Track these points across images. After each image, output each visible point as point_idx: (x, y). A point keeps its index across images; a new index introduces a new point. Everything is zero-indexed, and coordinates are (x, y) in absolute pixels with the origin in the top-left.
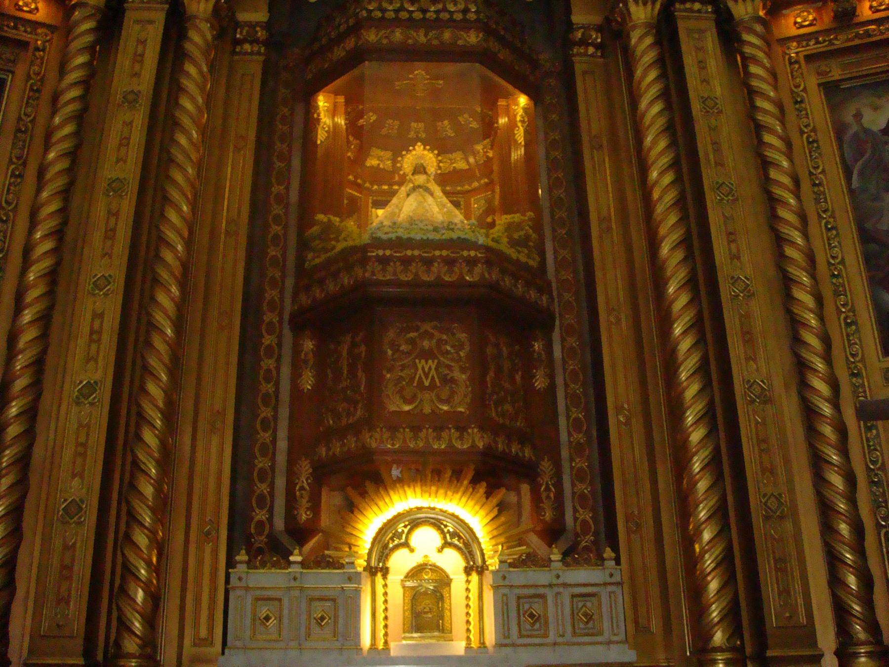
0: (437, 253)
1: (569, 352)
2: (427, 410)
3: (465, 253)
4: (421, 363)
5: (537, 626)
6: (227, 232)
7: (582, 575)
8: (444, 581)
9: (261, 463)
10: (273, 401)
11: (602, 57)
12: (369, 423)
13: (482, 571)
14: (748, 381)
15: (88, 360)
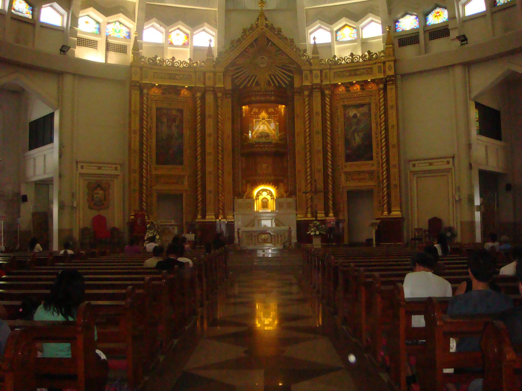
8: (268, 200)
11: (300, 95)
13: (273, 199)
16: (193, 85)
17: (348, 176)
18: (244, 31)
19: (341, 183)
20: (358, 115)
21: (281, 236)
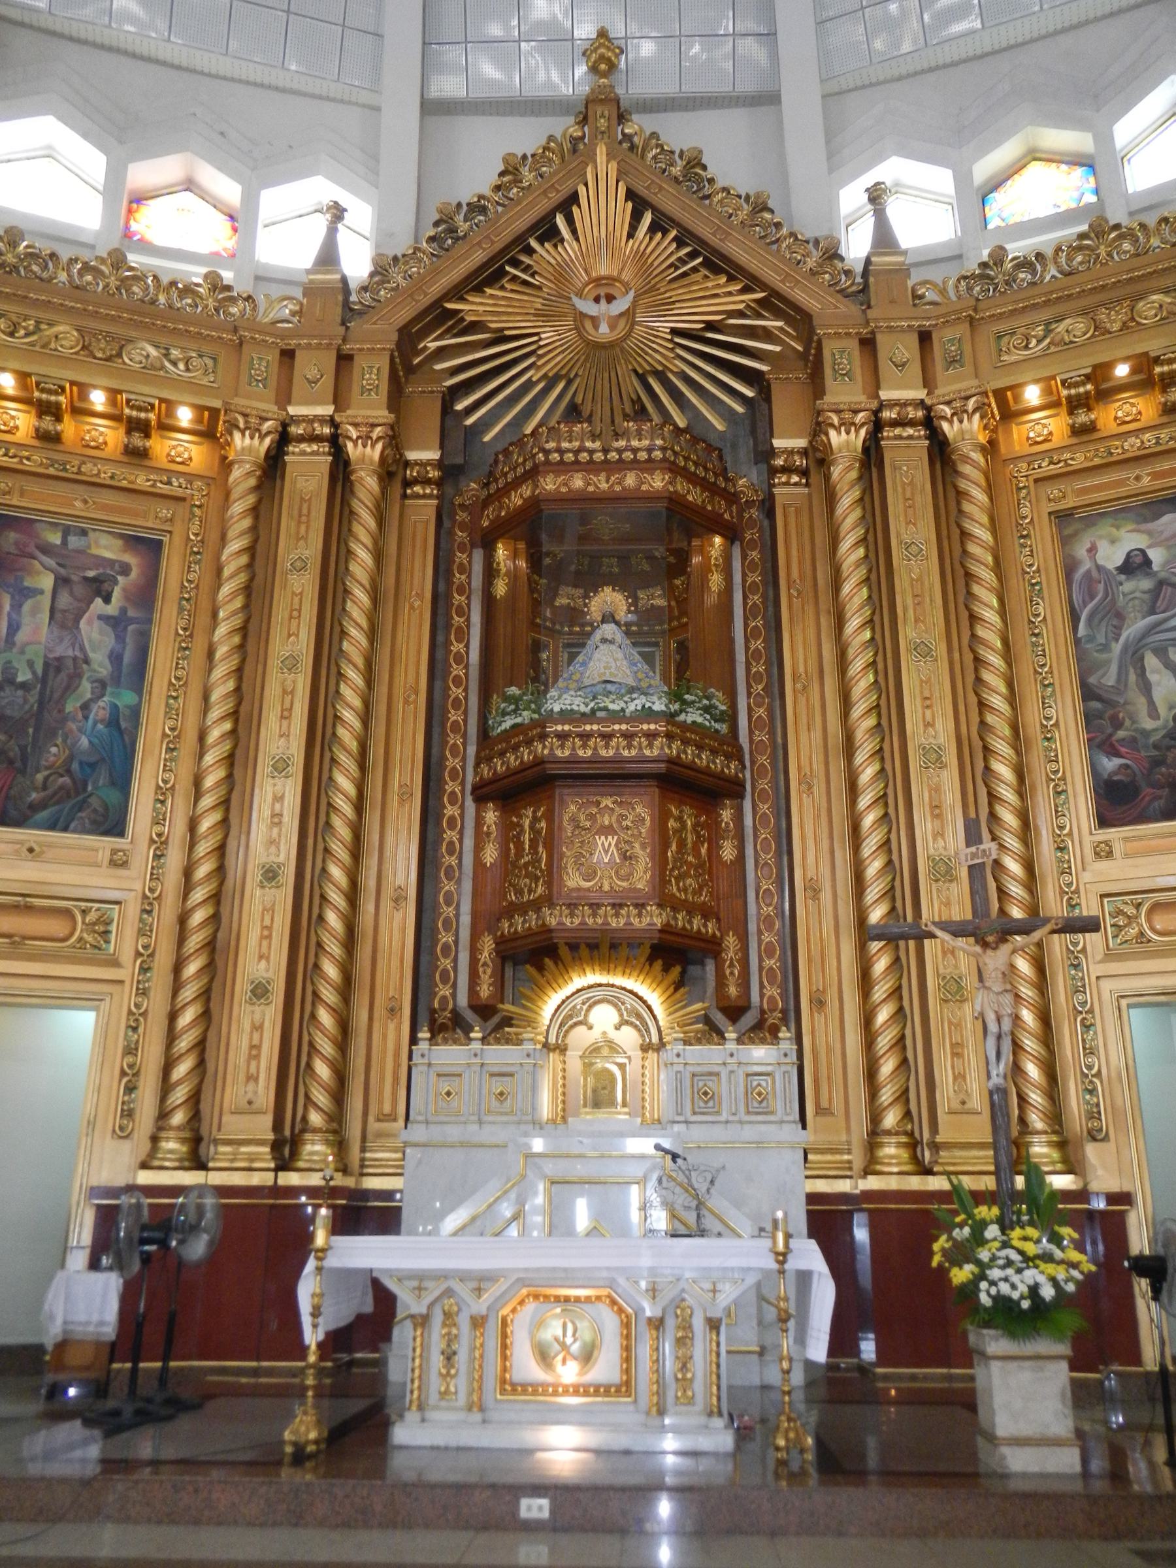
0: (617, 727)
1: (760, 820)
2: (606, 888)
3: (645, 727)
4: (600, 840)
5: (711, 1104)
6: (406, 702)
7: (760, 1053)
9: (446, 938)
10: (457, 874)
11: (807, 485)
12: (548, 901)
14: (934, 859)
15: (272, 842)
16: (217, 403)
17: (1131, 911)
18: (511, 170)
19: (1084, 950)
20: (1156, 556)
21: (714, 1325)
